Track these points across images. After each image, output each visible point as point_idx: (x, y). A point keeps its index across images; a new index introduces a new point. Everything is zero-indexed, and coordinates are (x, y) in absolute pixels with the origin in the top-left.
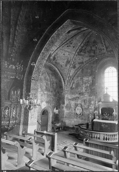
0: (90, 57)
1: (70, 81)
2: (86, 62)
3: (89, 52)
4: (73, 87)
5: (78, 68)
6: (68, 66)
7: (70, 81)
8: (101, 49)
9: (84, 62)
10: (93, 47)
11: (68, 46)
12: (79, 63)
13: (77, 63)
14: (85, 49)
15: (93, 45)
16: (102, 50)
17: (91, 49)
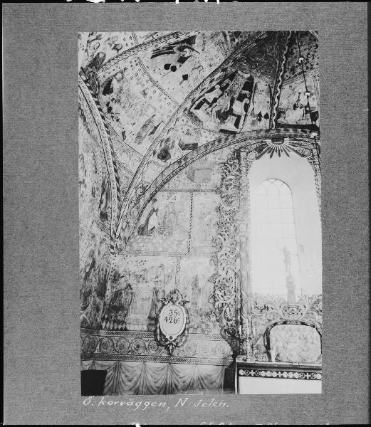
0: (223, 136)
1: (142, 203)
2: (206, 146)
3: (222, 116)
4: (150, 227)
5: (179, 162)
6: (143, 144)
7: (142, 203)
8: (260, 115)
9: (199, 145)
10: (237, 102)
11: (167, 67)
12: (184, 147)
13: (177, 142)
14: (215, 100)
15: (240, 94)
16: (260, 120)
17: (231, 110)
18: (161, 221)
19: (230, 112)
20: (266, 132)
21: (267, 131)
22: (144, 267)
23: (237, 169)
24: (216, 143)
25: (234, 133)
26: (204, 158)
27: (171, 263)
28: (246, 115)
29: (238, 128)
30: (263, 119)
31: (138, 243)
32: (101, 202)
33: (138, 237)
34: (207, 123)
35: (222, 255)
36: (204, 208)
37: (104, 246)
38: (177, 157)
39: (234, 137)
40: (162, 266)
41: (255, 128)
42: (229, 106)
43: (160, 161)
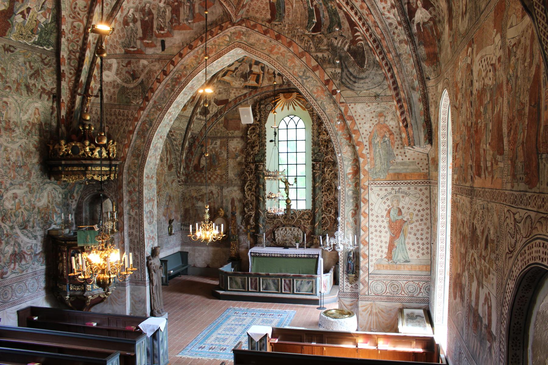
2: (235, 100)
8: (274, 73)
9: (230, 100)
16: (275, 77)
18: (208, 161)
19: (251, 72)
20: (280, 86)
21: (281, 86)
22: (201, 193)
23: (258, 119)
24: (243, 97)
25: (255, 88)
26: (234, 109)
27: (217, 190)
28: (263, 74)
29: (258, 83)
30: (277, 76)
31: (195, 178)
32: (167, 160)
33: (195, 173)
34: (234, 83)
35: (248, 186)
36: (236, 151)
37: (174, 184)
38: (214, 111)
39: (256, 91)
40: (212, 192)
41: (271, 83)
42: (249, 69)
43: (202, 117)
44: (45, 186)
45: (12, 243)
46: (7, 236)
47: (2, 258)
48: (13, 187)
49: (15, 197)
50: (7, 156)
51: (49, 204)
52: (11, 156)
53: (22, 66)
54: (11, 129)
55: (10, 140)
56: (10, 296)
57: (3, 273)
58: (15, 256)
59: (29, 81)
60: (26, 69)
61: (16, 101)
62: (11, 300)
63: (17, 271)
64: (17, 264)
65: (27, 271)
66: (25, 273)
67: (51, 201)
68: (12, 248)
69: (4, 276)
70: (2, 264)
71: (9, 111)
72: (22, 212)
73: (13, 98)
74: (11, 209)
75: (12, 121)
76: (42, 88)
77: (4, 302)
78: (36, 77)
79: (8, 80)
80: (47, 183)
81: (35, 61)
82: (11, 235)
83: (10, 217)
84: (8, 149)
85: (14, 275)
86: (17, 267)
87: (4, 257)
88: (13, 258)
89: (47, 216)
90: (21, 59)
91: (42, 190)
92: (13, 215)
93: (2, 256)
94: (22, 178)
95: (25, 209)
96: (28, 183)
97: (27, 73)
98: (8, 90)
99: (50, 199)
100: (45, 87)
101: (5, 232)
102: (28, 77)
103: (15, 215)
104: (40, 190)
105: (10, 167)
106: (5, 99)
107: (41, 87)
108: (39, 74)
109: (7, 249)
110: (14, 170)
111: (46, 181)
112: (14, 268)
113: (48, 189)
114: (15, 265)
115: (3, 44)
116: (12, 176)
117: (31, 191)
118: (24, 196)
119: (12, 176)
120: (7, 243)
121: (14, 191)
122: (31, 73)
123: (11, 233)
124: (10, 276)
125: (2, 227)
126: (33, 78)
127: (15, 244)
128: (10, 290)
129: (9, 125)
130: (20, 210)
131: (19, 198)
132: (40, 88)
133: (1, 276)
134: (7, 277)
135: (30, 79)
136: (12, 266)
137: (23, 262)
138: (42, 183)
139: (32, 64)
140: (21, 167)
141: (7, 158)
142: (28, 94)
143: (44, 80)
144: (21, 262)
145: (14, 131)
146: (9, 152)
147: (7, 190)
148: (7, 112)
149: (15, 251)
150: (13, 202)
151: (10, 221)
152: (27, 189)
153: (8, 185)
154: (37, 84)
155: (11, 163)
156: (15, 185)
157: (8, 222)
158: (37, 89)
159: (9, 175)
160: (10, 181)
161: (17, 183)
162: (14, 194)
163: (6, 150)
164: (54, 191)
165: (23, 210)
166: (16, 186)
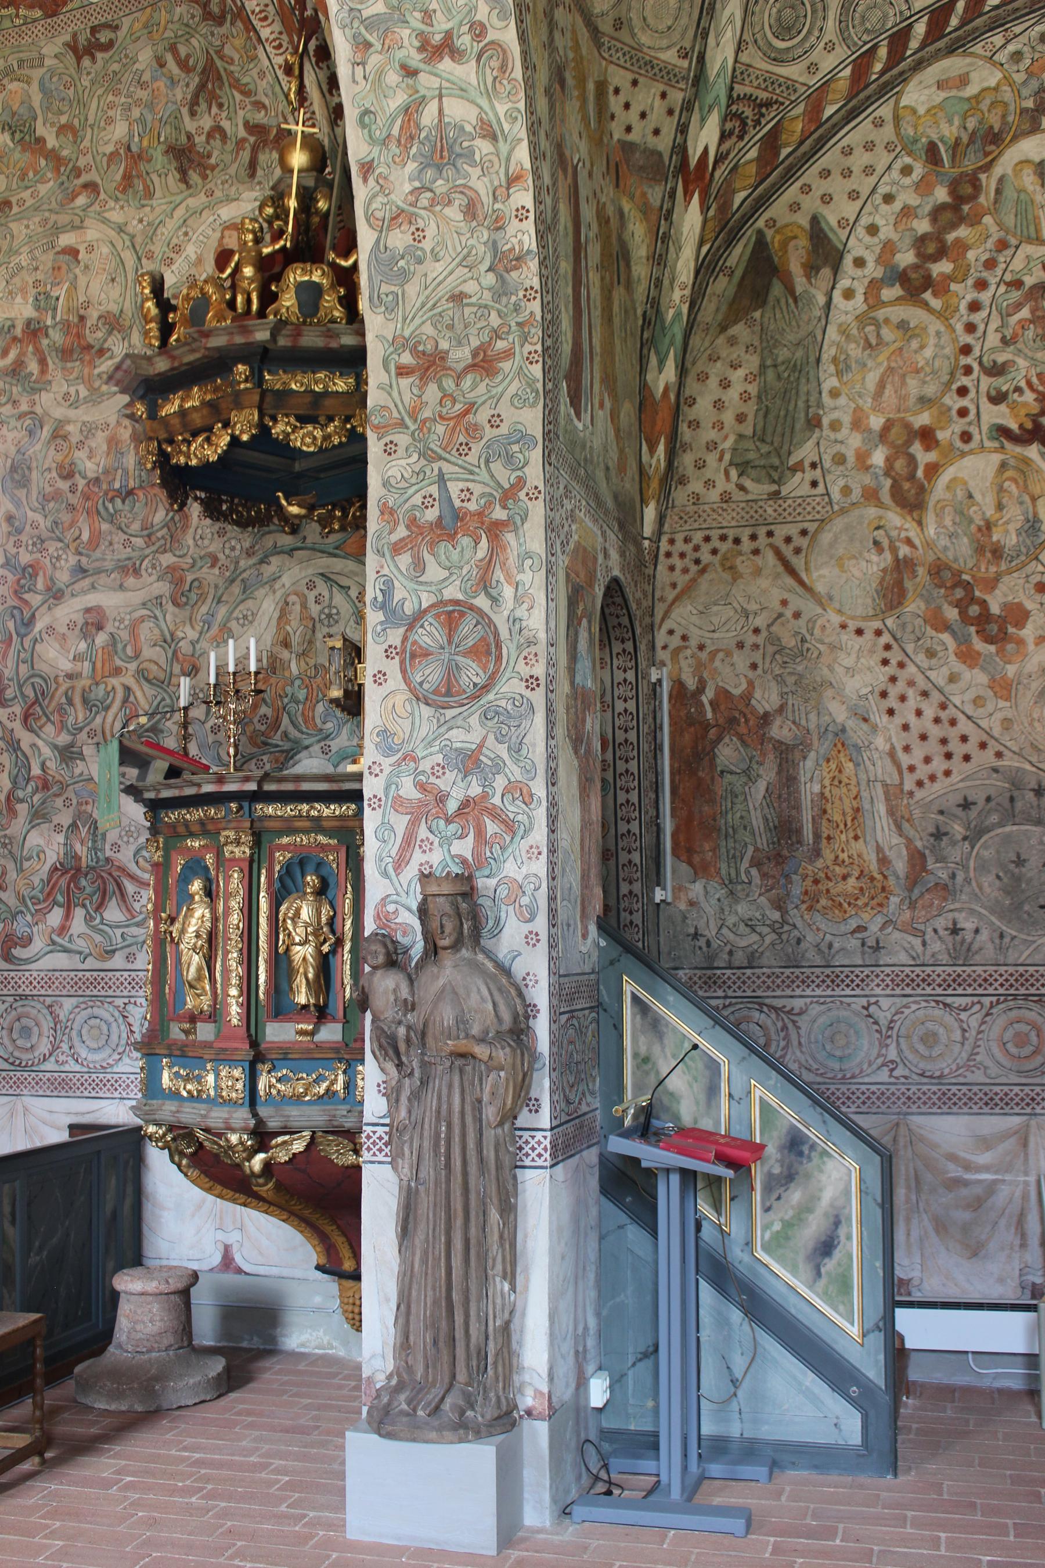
44: (268, 570)
45: (65, 819)
46: (45, 785)
47: (12, 875)
48: (86, 583)
49: (94, 622)
50: (59, 457)
51: (285, 654)
52: (81, 455)
53: (154, 79)
54: (90, 347)
55: (83, 392)
56: (44, 1048)
57: (12, 941)
58: (74, 879)
59: (189, 125)
60: (173, 82)
61: (121, 229)
62: (50, 1065)
63: (81, 944)
64: (79, 913)
65: (130, 958)
66: (118, 961)
67: (295, 640)
68: (61, 838)
69: (17, 952)
70: (9, 897)
71: (82, 281)
72: (128, 689)
73: (105, 221)
74: (70, 676)
75: (93, 315)
76: (252, 128)
77: (18, 1065)
78: (213, 99)
79: (81, 163)
80: (277, 551)
81: (189, 31)
82: (64, 787)
83: (61, 710)
84: (70, 428)
85: (61, 960)
86: (78, 924)
87: (20, 870)
88: (63, 882)
89: (264, 710)
90: (145, 57)
91: (246, 588)
92: (77, 700)
93: (11, 866)
94: (139, 542)
95: (142, 674)
96: (167, 559)
97: (179, 97)
98: (81, 200)
99: (296, 630)
100: (260, 117)
101: (36, 771)
102: (185, 111)
103: (85, 701)
104: (236, 589)
105: (74, 500)
106: (66, 240)
107: (246, 124)
108: (219, 78)
109: (35, 839)
110: (93, 513)
111: (269, 541)
112: (63, 929)
113: (286, 580)
114: (68, 916)
115: (68, 38)
116: (85, 536)
117: (183, 593)
118: (142, 619)
119: (85, 536)
120: (39, 816)
121: (92, 599)
122: (193, 86)
123: (64, 774)
124: (43, 960)
125: (25, 746)
126: (203, 106)
127: (74, 825)
128: (47, 1023)
129: (78, 335)
130: (114, 681)
131: (109, 628)
132: (242, 133)
133: (4, 947)
134: (28, 961)
135: (193, 114)
136: (55, 917)
137: (113, 913)
138: (249, 553)
139: (183, 51)
140: (130, 493)
141: (60, 467)
142: (184, 179)
143: (247, 93)
144: (100, 907)
145: (101, 352)
146: (74, 439)
147: (56, 595)
148: (74, 286)
149: (77, 858)
150: (83, 646)
151: (62, 726)
152: (163, 588)
153: (63, 577)
154: (226, 124)
155: (81, 483)
156: (99, 572)
157: (49, 729)
158: (230, 146)
159: (73, 533)
160: (73, 560)
161: (109, 565)
162: (88, 610)
163: (58, 435)
164: (322, 588)
165: (131, 682)
166: (103, 579)
